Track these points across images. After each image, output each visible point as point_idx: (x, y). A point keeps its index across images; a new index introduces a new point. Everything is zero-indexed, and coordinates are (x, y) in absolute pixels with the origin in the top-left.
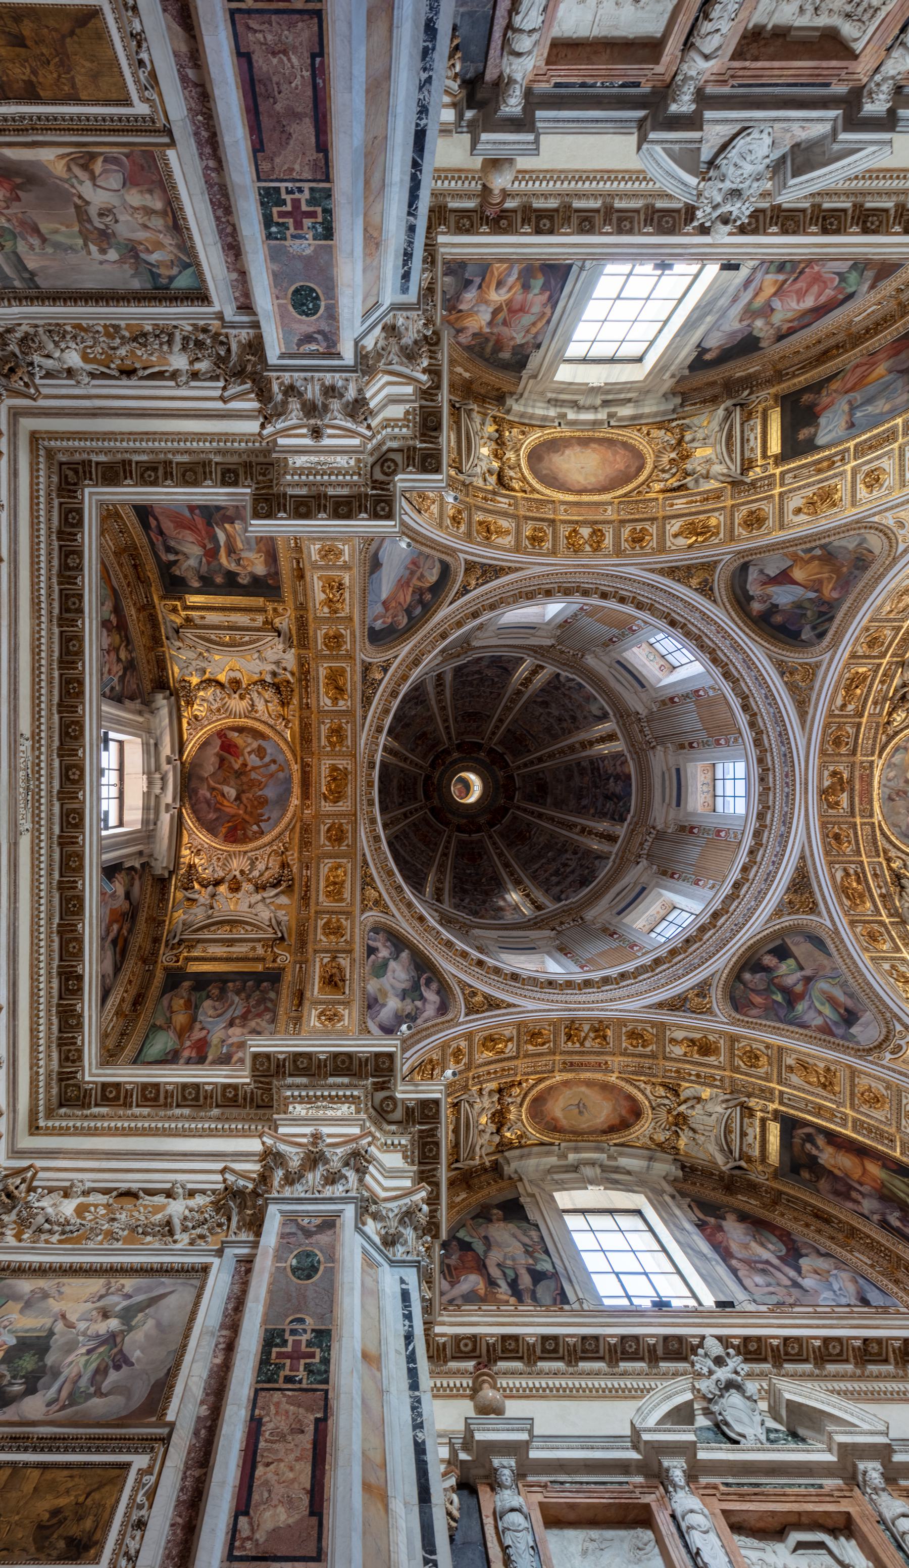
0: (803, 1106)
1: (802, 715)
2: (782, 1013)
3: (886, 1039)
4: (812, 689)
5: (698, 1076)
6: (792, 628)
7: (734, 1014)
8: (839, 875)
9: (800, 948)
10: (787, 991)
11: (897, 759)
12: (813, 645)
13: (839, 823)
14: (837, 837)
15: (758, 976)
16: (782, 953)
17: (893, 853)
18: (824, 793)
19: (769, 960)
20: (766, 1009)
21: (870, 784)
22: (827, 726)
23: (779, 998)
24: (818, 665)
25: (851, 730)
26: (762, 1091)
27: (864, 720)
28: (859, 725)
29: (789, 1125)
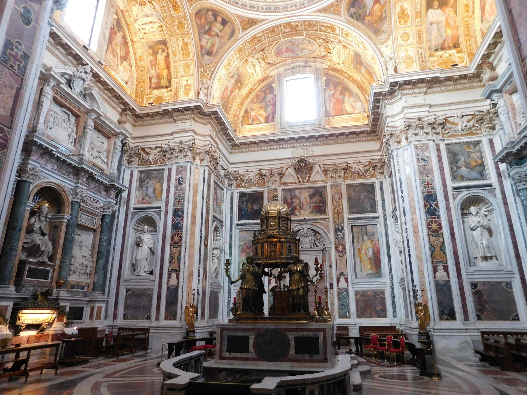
0: (173, 47)
1: (320, 11)
2: (202, 31)
3: (207, 68)
4: (330, 13)
5: (163, 6)
6: (356, 4)
7: (194, 14)
8: (260, 35)
9: (228, 29)
10: (210, 29)
11: (305, 41)
12: (348, 13)
13: (278, 30)
14: (273, 31)
15: (212, 17)
16: (224, 22)
17: (271, 47)
18: (289, 24)
19: (219, 19)
20: (201, 25)
21: (295, 36)
22: (316, 22)
23: (207, 27)
24: (340, 15)
25: (314, 29)
26: (171, 32)
27: (319, 32)
28: (317, 30)
29: (164, 43)
